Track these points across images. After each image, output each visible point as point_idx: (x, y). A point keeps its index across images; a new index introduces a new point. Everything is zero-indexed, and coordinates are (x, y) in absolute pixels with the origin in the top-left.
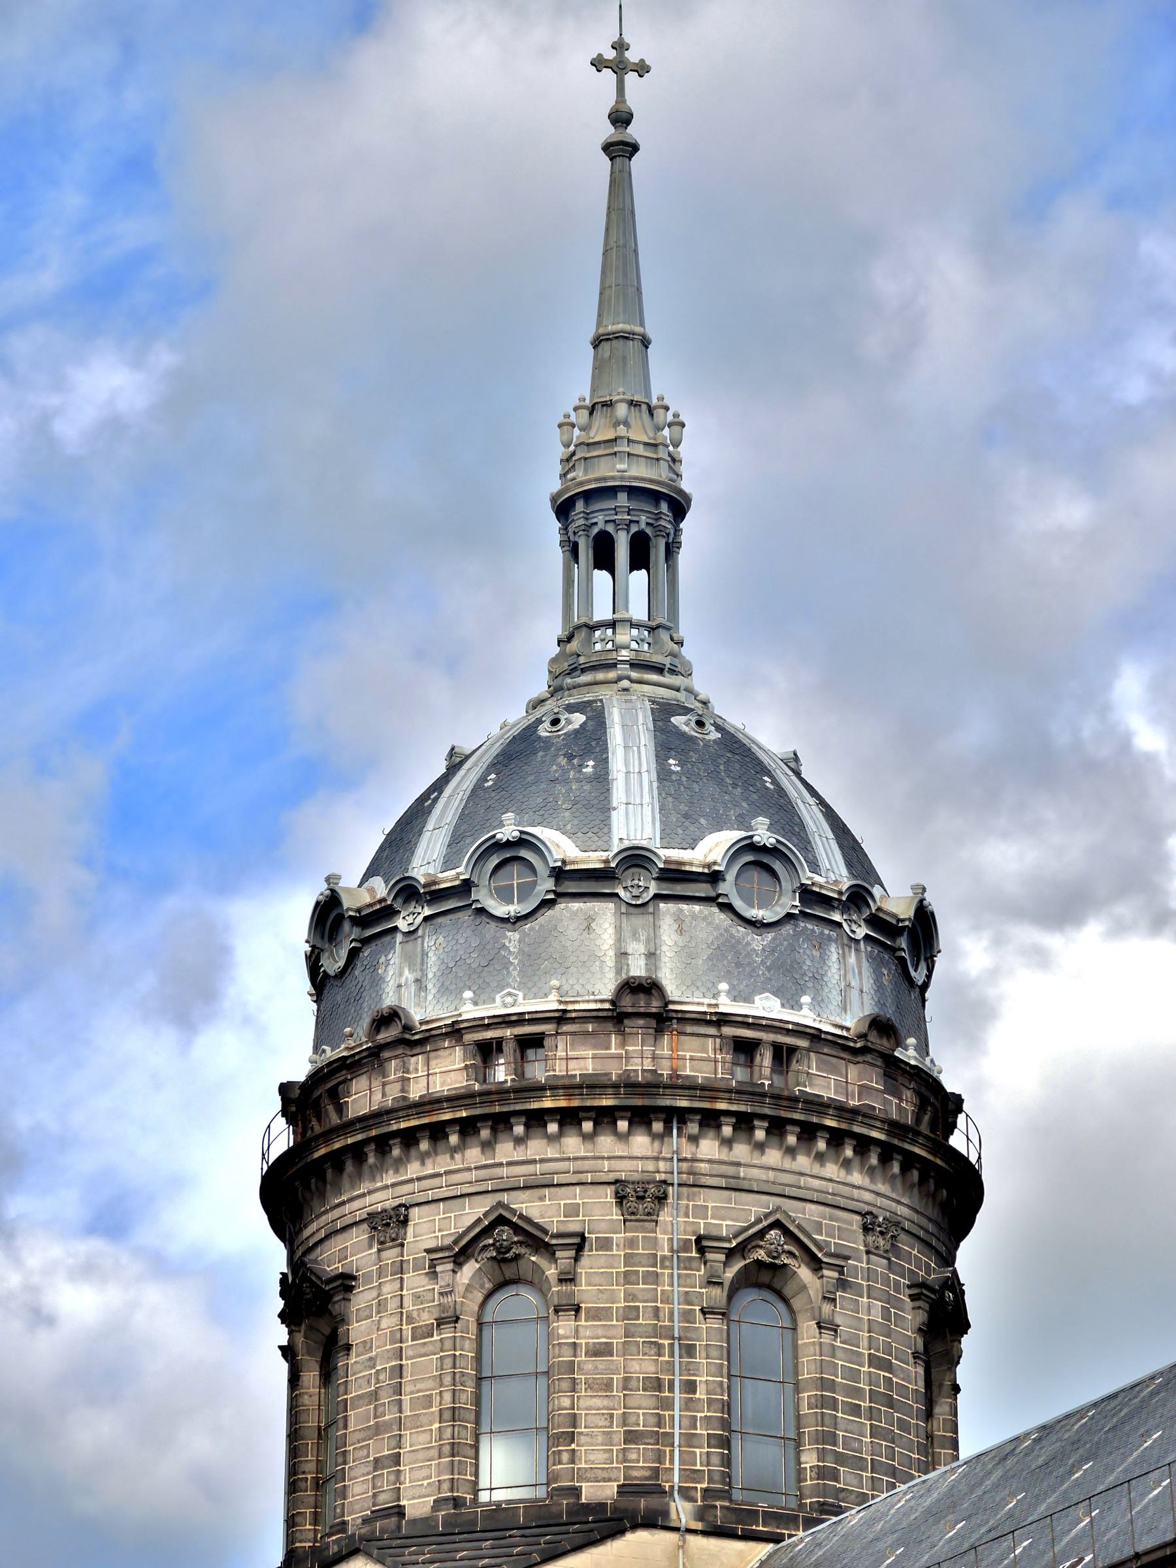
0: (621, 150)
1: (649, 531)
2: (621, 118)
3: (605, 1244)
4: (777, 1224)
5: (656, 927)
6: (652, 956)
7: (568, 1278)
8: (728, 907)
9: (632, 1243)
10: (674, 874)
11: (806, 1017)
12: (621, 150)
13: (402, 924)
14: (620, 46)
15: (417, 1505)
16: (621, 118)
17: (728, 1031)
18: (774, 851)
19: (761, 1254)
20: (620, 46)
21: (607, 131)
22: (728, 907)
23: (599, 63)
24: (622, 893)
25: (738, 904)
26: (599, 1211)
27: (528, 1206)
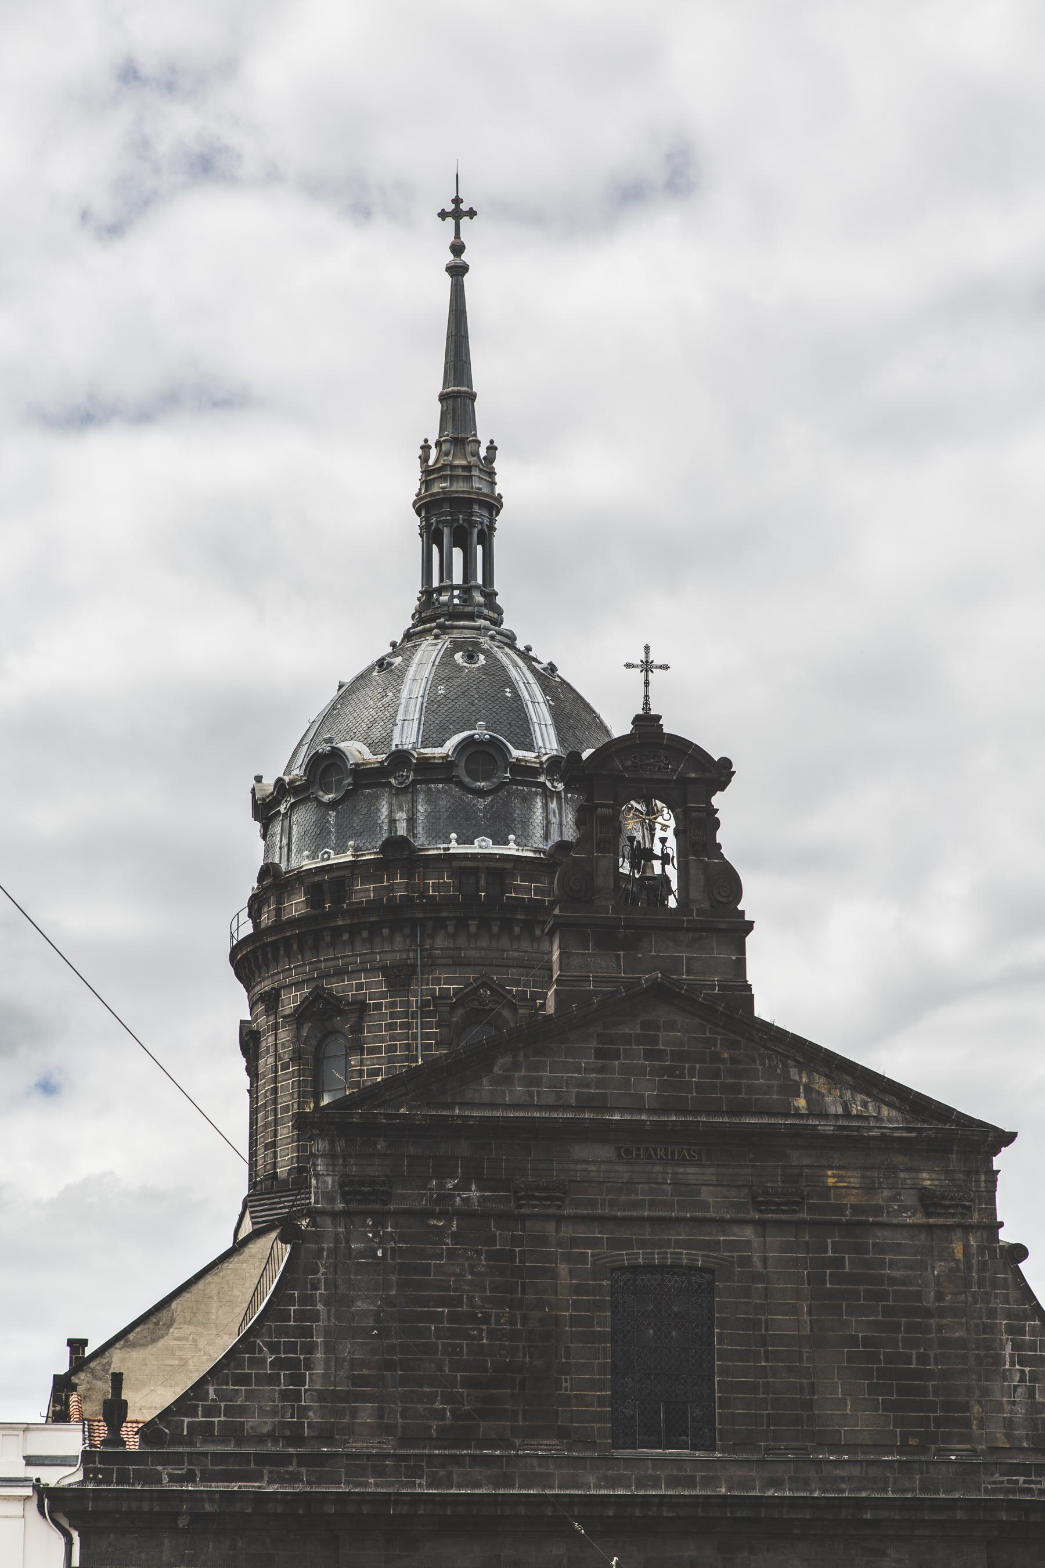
0: (457, 271)
1: (465, 525)
2: (457, 249)
3: (378, 1007)
4: (484, 985)
5: (414, 802)
6: (411, 821)
7: (357, 1029)
8: (460, 784)
9: (393, 1005)
10: (426, 765)
11: (511, 849)
12: (457, 271)
13: (282, 809)
14: (457, 201)
15: (282, 1171)
16: (457, 249)
17: (455, 864)
18: (493, 742)
19: (476, 1005)
20: (457, 201)
21: (451, 257)
22: (460, 784)
23: (443, 215)
24: (393, 781)
25: (467, 780)
26: (370, 987)
27: (335, 986)
